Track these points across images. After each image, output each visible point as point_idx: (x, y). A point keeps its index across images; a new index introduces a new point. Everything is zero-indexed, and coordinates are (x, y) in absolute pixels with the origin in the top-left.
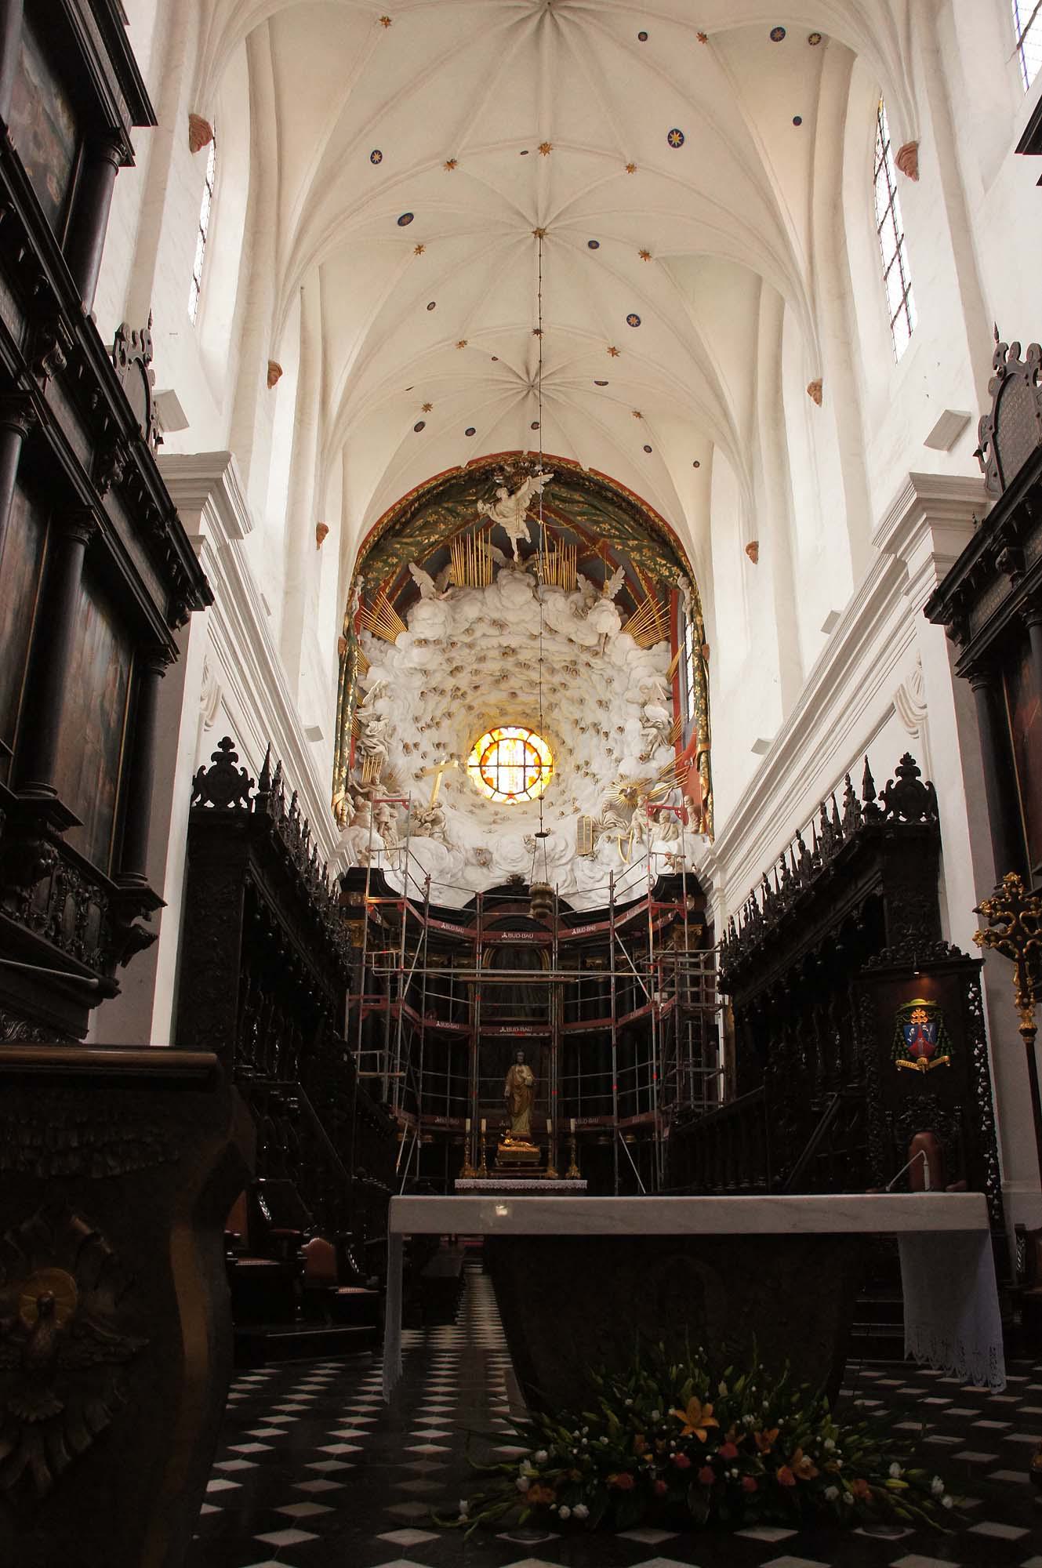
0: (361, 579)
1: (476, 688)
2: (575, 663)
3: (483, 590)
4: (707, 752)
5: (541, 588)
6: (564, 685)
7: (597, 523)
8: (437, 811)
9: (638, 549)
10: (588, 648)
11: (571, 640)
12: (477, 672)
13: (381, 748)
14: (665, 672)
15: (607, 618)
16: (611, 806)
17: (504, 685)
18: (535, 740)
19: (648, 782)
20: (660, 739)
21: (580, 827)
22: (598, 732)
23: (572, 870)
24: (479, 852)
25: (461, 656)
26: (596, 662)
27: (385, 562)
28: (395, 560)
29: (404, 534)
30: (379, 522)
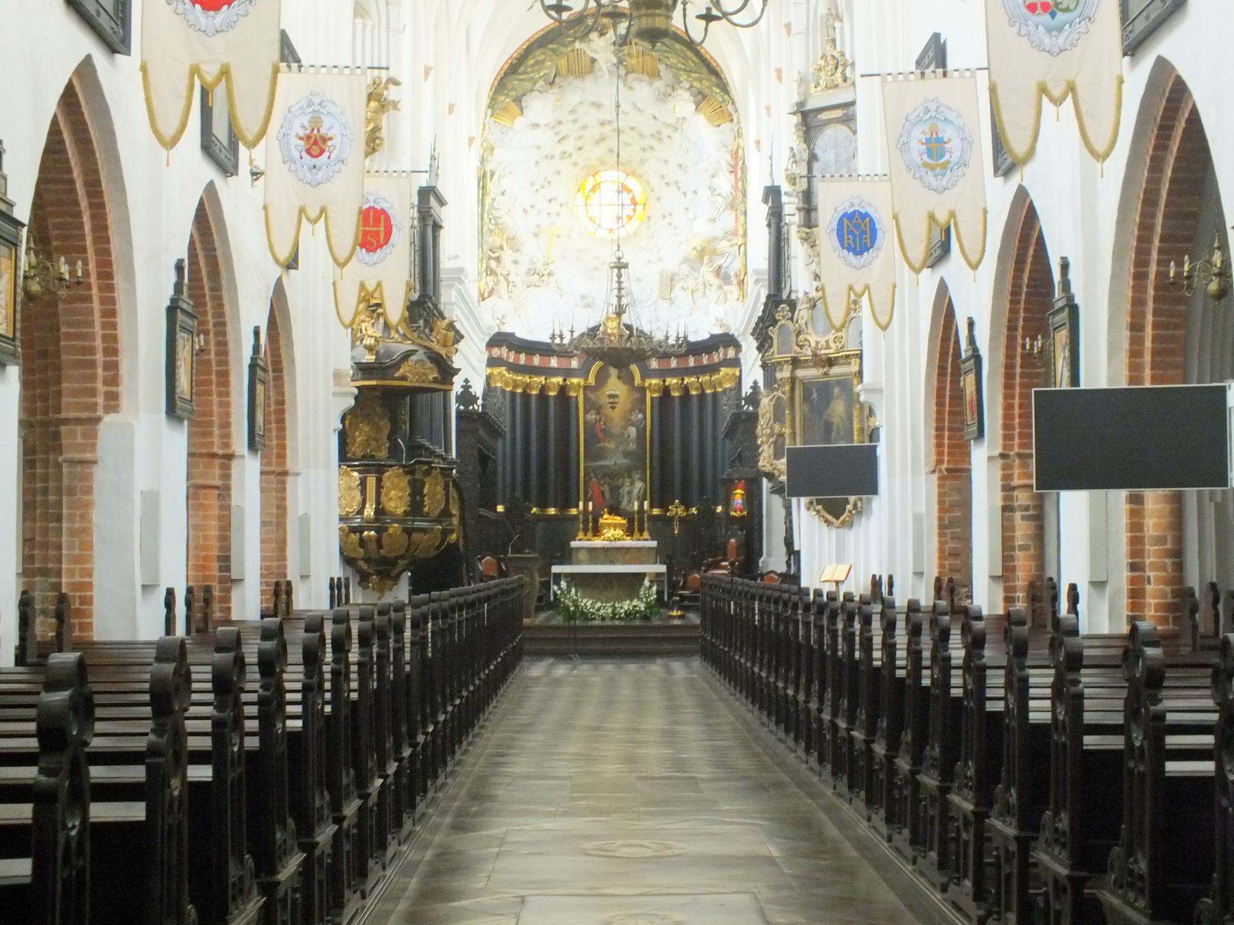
0: (490, 111)
1: (580, 149)
2: (659, 133)
3: (583, 79)
4: (745, 244)
5: (631, 77)
6: (652, 148)
7: (668, 58)
8: (551, 267)
9: (700, 80)
10: (669, 125)
11: (655, 118)
12: (580, 138)
13: (506, 219)
14: (730, 148)
15: (683, 103)
16: (686, 260)
17: (603, 145)
18: (632, 182)
19: (715, 239)
20: (724, 205)
21: (661, 277)
22: (679, 189)
23: (656, 310)
24: (583, 297)
25: (563, 130)
26: (677, 136)
27: (507, 95)
28: (514, 93)
29: (520, 71)
30: (502, 69)
